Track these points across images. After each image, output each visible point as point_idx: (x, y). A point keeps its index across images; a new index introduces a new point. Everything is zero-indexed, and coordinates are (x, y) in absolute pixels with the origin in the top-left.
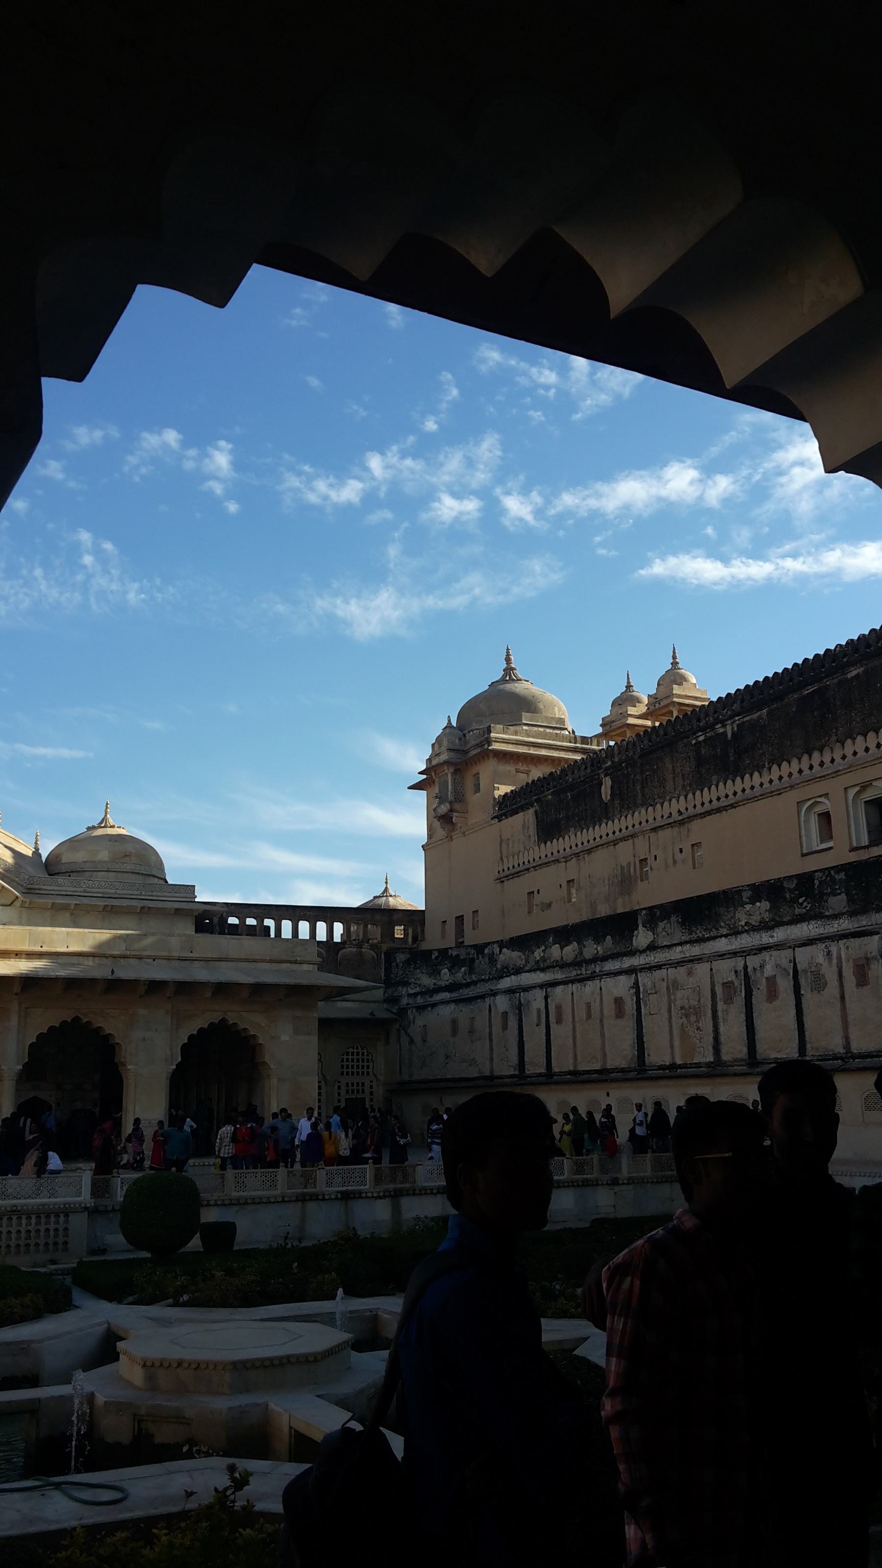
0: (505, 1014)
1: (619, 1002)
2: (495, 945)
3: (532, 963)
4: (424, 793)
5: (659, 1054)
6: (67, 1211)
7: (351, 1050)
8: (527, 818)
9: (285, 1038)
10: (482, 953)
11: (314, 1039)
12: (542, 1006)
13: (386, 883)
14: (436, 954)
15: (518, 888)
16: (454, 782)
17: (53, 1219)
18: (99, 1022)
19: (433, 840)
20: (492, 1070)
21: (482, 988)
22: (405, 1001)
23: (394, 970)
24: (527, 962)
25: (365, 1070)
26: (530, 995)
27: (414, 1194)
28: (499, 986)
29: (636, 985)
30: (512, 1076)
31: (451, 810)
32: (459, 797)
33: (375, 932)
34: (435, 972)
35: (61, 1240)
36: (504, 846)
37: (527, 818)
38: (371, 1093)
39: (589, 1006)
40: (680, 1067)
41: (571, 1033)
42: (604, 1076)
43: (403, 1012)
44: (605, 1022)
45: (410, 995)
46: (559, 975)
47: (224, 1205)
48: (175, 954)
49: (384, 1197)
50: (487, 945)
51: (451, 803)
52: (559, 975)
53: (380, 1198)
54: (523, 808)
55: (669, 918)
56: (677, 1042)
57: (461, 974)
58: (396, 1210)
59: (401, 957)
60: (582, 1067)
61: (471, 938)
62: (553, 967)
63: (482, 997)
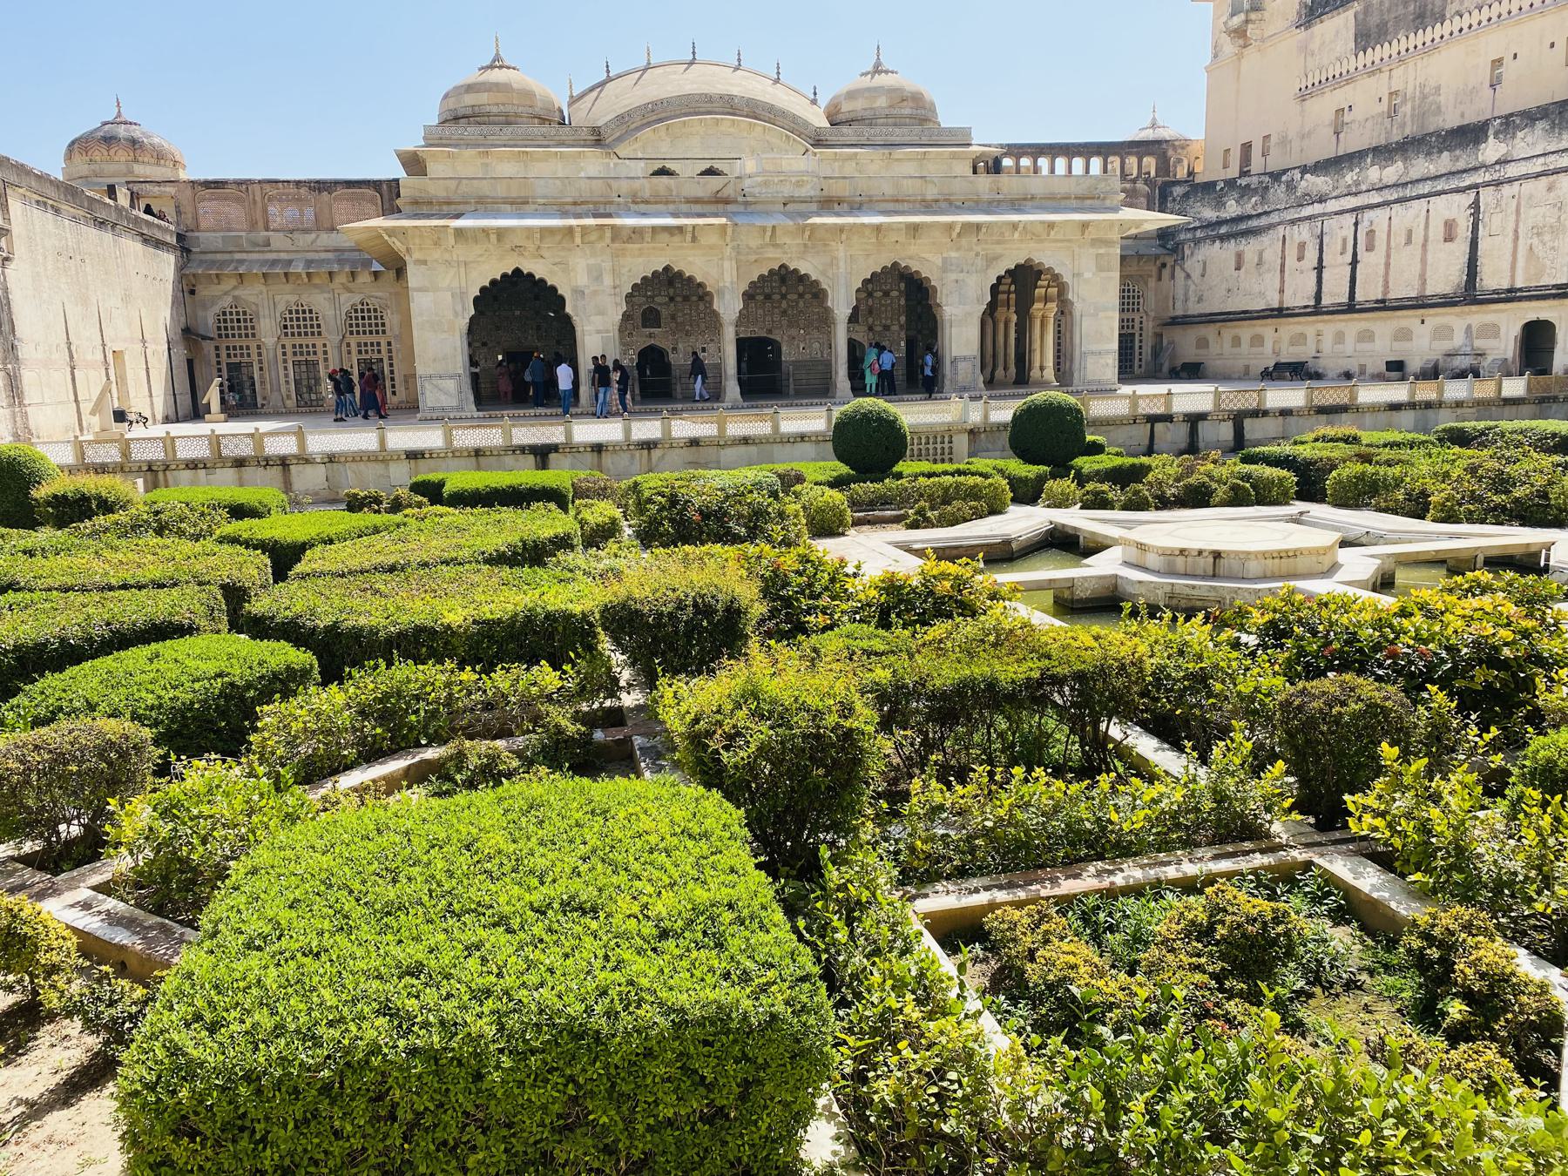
1: (1450, 226)
5: (1492, 277)
15: (1323, 107)
20: (1281, 302)
21: (1274, 218)
29: (1476, 205)
31: (1247, 21)
33: (1150, 163)
34: (1220, 204)
39: (1410, 233)
40: (1520, 290)
41: (1383, 261)
42: (1420, 303)
44: (1430, 247)
46: (1375, 198)
50: (1285, 172)
55: (1533, 126)
56: (1521, 263)
60: (1391, 296)
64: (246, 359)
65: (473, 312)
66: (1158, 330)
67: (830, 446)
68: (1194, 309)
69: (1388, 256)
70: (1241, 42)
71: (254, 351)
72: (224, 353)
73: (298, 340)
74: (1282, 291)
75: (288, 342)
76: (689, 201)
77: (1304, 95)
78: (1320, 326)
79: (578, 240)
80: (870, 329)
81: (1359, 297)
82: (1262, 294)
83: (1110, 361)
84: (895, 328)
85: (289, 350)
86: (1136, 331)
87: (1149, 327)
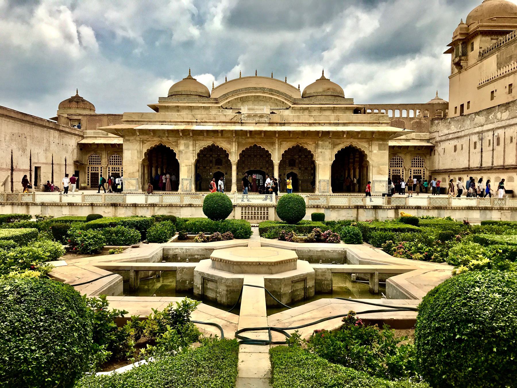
2: (473, 115)
4: (449, 56)
6: (268, 207)
9: (375, 152)
11: (387, 152)
13: (437, 94)
16: (462, 48)
18: (305, 146)
20: (469, 165)
22: (438, 139)
26: (485, 134)
31: (460, 60)
32: (465, 54)
35: (266, 216)
38: (424, 174)
39: (512, 138)
41: (503, 150)
47: (326, 208)
51: (460, 57)
58: (397, 213)
64: (97, 172)
65: (144, 158)
67: (202, 208)
69: (504, 148)
70: (460, 67)
71: (100, 169)
72: (90, 170)
74: (469, 161)
75: (111, 167)
76: (221, 122)
77: (479, 88)
79: (181, 134)
80: (300, 169)
83: (385, 185)
84: (309, 169)
85: (111, 169)
87: (427, 173)
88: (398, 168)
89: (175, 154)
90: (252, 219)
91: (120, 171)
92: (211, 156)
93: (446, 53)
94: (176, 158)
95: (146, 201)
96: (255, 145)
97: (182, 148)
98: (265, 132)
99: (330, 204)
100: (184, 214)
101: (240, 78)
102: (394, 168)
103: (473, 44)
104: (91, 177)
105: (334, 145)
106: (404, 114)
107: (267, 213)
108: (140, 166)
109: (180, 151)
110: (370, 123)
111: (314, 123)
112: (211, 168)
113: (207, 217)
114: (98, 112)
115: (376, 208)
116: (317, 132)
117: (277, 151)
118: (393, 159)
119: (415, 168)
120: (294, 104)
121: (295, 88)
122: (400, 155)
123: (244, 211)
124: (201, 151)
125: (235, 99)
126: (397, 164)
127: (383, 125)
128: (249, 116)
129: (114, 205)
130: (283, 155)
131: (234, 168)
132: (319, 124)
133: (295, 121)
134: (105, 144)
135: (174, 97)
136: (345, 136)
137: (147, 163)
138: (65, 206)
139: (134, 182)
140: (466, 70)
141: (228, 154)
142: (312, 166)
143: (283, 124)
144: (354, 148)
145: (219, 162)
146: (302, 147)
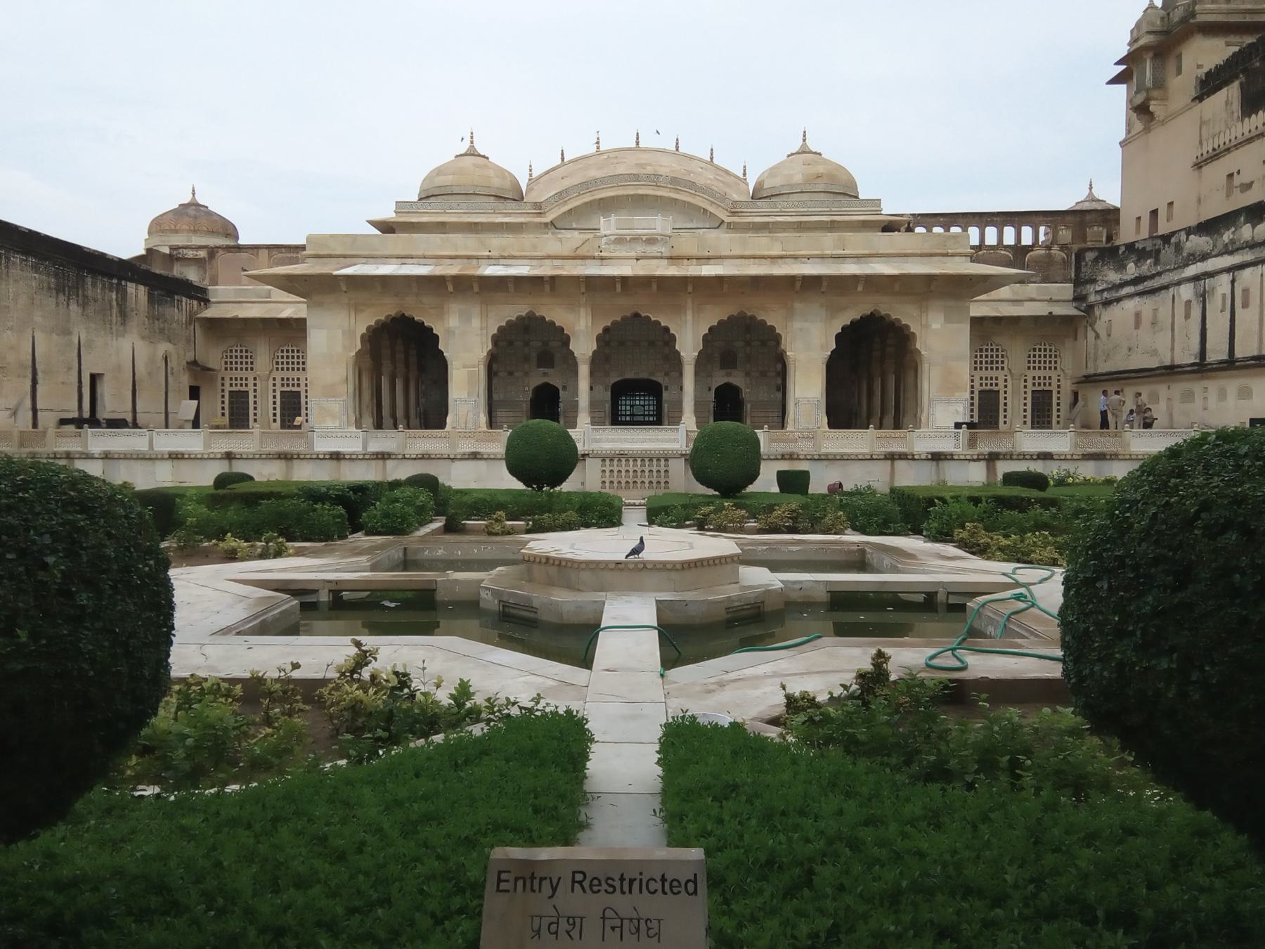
0: (1188, 303)
3: (1220, 246)
4: (1122, 89)
6: (666, 457)
7: (1037, 347)
8: (1231, 93)
10: (1169, 243)
11: (966, 328)
12: (1228, 292)
13: (1091, 188)
14: (1122, 249)
16: (1154, 69)
17: (655, 462)
19: (1133, 133)
20: (1172, 360)
23: (1083, 270)
24: (1215, 246)
25: (1053, 365)
27: (1011, 459)
28: (1183, 275)
30: (1193, 365)
31: (1148, 99)
32: (1159, 84)
33: (1065, 235)
34: (1122, 267)
35: (663, 480)
36: (1204, 128)
37: (1231, 93)
41: (1257, 318)
43: (1091, 307)
45: (1097, 292)
46: (1248, 256)
48: (828, 252)
49: (978, 460)
52: (1248, 256)
53: (974, 460)
54: (1226, 83)
57: (1147, 266)
58: (991, 470)
59: (1090, 256)
61: (1163, 229)
62: (1242, 248)
63: (1166, 287)
64: (243, 389)
65: (359, 347)
66: (1074, 387)
68: (1104, 367)
71: (251, 382)
72: (227, 382)
73: (286, 374)
74: (1173, 349)
75: (278, 375)
76: (549, 257)
77: (1198, 166)
78: (1205, 383)
79: (451, 288)
80: (748, 374)
81: (1239, 354)
82: (1155, 352)
85: (278, 382)
86: (1054, 388)
87: (1067, 386)
88: (994, 373)
89: (437, 337)
90: (627, 488)
91: (303, 385)
92: (527, 344)
93: (1116, 80)
94: (440, 347)
95: (365, 447)
96: (637, 315)
97: (453, 321)
98: (662, 281)
99: (824, 451)
100: (459, 477)
101: (599, 153)
102: (984, 373)
103: (1179, 57)
104: (231, 403)
105: (833, 311)
106: (1009, 236)
107: (666, 471)
108: (351, 369)
109: (449, 332)
110: (922, 255)
111: (781, 257)
112: (527, 374)
113: (518, 485)
114: (242, 241)
115: (937, 457)
116: (791, 279)
117: (689, 325)
118: (981, 350)
119: (1037, 373)
120: (734, 214)
121: (737, 177)
122: (998, 340)
123: (607, 469)
124: (500, 329)
125: (586, 203)
126: (992, 362)
127: (957, 259)
128: (620, 240)
129: (286, 457)
130: (705, 337)
131: (584, 370)
132: (795, 257)
133: (736, 252)
134: (263, 320)
135: (432, 200)
136: (860, 288)
137: (368, 362)
138: (162, 459)
139: (335, 407)
140: (1163, 123)
141: (568, 338)
142: (779, 366)
143: (708, 259)
144: (882, 318)
145: (546, 360)
146: (753, 318)
